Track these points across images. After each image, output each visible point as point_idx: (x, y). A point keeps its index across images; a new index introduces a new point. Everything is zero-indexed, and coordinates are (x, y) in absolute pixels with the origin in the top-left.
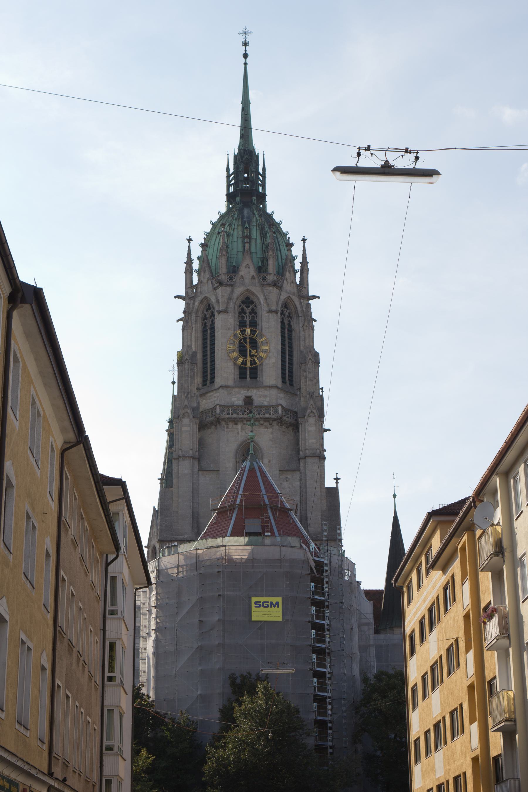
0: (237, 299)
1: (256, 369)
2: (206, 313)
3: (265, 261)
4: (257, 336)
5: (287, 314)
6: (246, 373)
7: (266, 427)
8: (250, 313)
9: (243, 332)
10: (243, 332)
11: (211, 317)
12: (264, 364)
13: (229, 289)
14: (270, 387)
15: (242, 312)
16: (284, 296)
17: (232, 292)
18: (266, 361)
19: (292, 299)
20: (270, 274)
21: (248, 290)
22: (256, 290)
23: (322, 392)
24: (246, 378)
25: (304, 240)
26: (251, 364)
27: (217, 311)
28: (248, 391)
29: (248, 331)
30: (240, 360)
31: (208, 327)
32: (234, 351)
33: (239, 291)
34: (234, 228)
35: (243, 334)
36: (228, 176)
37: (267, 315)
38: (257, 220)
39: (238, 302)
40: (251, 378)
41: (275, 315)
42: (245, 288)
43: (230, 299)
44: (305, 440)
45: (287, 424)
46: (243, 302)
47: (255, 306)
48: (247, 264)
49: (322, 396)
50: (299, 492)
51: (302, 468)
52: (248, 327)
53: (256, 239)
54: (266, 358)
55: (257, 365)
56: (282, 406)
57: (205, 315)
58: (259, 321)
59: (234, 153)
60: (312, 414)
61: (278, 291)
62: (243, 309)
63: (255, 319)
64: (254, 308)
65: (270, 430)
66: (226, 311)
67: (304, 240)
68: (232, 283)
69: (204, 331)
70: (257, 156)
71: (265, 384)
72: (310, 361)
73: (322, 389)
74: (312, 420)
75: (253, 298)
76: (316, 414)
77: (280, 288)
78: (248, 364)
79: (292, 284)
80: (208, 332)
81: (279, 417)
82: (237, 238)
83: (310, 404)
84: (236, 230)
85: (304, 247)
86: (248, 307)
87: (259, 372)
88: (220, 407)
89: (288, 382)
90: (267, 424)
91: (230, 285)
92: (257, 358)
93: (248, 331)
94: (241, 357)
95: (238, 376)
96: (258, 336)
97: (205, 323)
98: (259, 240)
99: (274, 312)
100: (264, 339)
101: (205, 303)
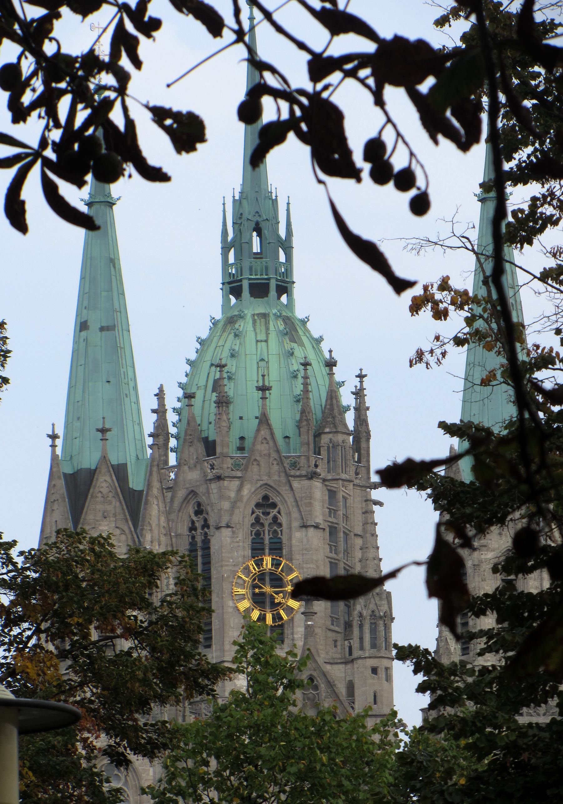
2: (195, 518)
4: (282, 570)
9: (259, 563)
10: (259, 563)
11: (203, 527)
26: (274, 619)
29: (268, 561)
30: (255, 614)
31: (199, 544)
46: (258, 505)
47: (279, 512)
52: (267, 551)
55: (283, 622)
57: (193, 522)
59: (234, 197)
62: (257, 519)
63: (280, 536)
70: (275, 202)
75: (274, 498)
78: (269, 620)
80: (200, 553)
86: (266, 514)
93: (268, 561)
94: (256, 608)
96: (285, 569)
97: (193, 537)
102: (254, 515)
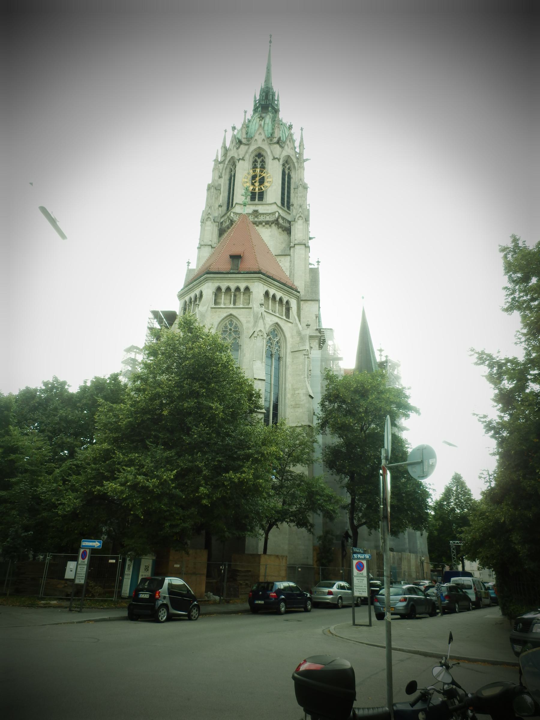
0: (252, 152)
1: (263, 193)
3: (273, 134)
5: (287, 167)
6: (255, 198)
7: (267, 228)
8: (261, 162)
10: (254, 171)
12: (268, 190)
13: (247, 147)
14: (271, 204)
15: (255, 161)
16: (285, 154)
17: (249, 148)
18: (270, 189)
19: (291, 158)
20: (276, 137)
21: (259, 148)
22: (265, 147)
23: (309, 206)
24: (255, 200)
25: (302, 129)
26: (259, 190)
27: (237, 159)
28: (256, 206)
29: (258, 170)
30: (251, 188)
32: (247, 182)
33: (253, 147)
34: (254, 119)
35: (254, 172)
36: (255, 101)
37: (272, 161)
38: (270, 116)
39: (253, 155)
40: (259, 200)
41: (277, 160)
42: (258, 146)
43: (246, 152)
44: (295, 236)
45: (282, 228)
46: (256, 156)
47: (265, 158)
48: (260, 133)
49: (308, 210)
50: (289, 270)
51: (292, 254)
53: (268, 124)
54: (270, 186)
56: (279, 213)
58: (266, 166)
60: (300, 218)
61: (281, 149)
64: (264, 158)
65: (270, 230)
66: (243, 159)
67: (302, 129)
68: (249, 143)
69: (230, 179)
71: (268, 202)
72: (301, 186)
73: (309, 205)
74: (300, 222)
75: (263, 153)
76: (304, 217)
77: (282, 147)
79: (291, 150)
81: (276, 219)
82: (256, 123)
83: (299, 211)
84: (255, 120)
85: (302, 133)
87: (265, 197)
88: (233, 214)
89: (286, 207)
90: (267, 226)
91: (247, 144)
92: (264, 187)
95: (250, 199)
97: (231, 174)
98: (270, 124)
99: (277, 158)
100: (269, 175)
101: (232, 161)
102: (254, 159)
